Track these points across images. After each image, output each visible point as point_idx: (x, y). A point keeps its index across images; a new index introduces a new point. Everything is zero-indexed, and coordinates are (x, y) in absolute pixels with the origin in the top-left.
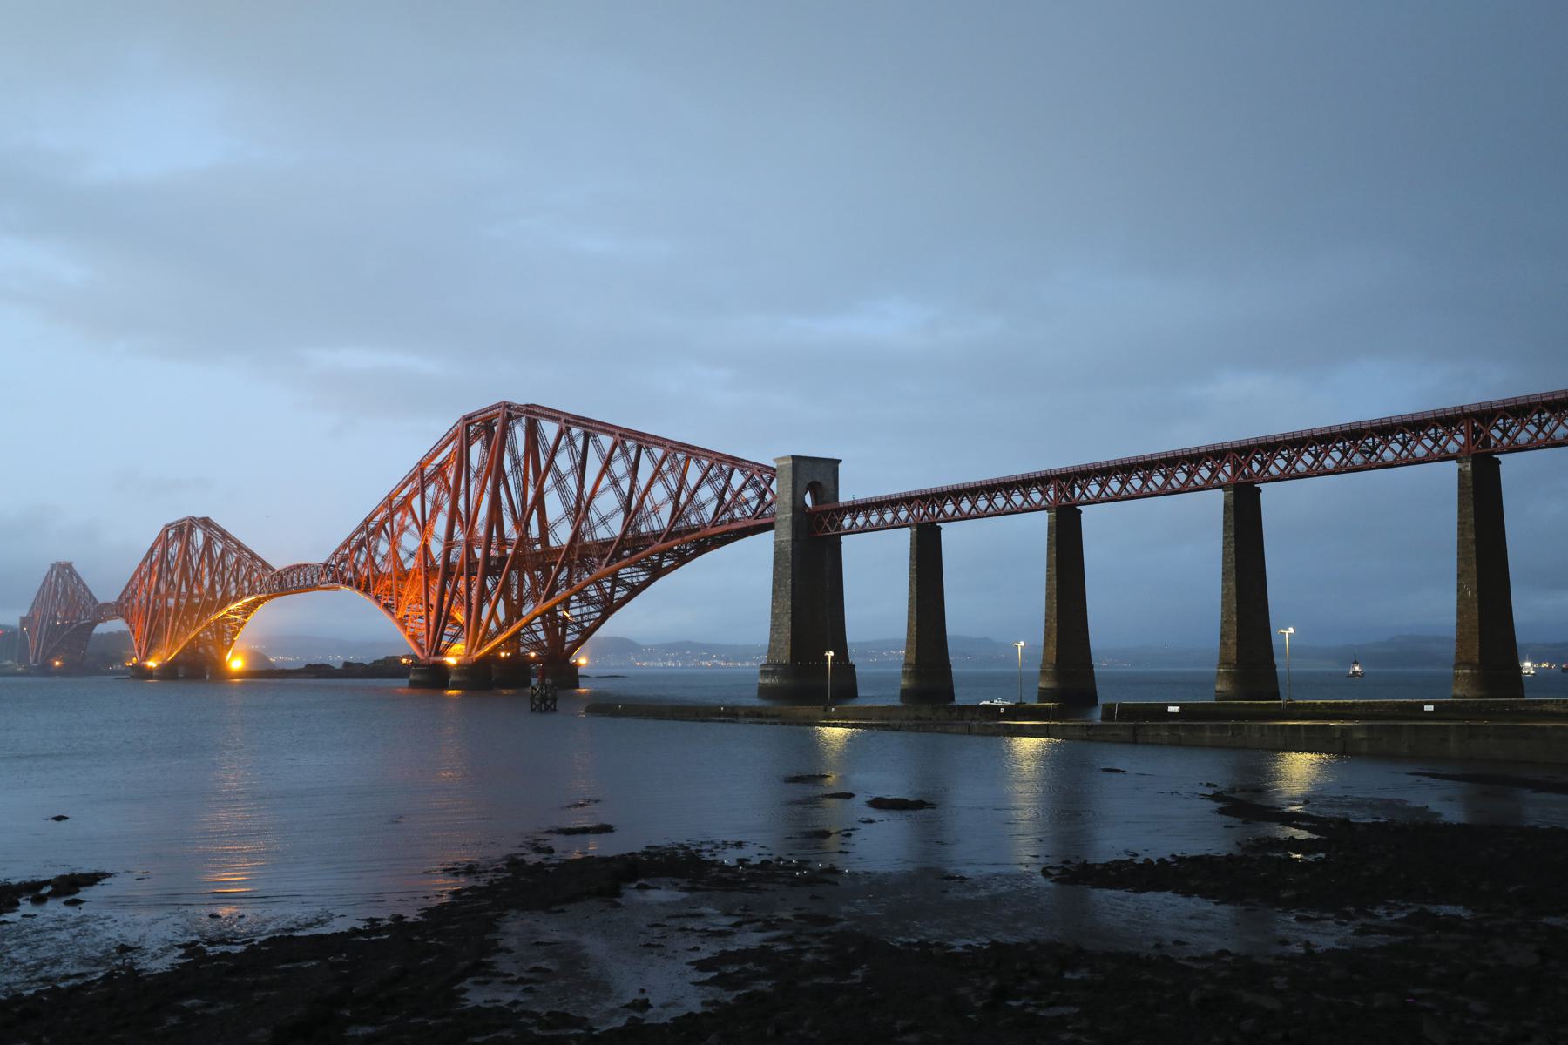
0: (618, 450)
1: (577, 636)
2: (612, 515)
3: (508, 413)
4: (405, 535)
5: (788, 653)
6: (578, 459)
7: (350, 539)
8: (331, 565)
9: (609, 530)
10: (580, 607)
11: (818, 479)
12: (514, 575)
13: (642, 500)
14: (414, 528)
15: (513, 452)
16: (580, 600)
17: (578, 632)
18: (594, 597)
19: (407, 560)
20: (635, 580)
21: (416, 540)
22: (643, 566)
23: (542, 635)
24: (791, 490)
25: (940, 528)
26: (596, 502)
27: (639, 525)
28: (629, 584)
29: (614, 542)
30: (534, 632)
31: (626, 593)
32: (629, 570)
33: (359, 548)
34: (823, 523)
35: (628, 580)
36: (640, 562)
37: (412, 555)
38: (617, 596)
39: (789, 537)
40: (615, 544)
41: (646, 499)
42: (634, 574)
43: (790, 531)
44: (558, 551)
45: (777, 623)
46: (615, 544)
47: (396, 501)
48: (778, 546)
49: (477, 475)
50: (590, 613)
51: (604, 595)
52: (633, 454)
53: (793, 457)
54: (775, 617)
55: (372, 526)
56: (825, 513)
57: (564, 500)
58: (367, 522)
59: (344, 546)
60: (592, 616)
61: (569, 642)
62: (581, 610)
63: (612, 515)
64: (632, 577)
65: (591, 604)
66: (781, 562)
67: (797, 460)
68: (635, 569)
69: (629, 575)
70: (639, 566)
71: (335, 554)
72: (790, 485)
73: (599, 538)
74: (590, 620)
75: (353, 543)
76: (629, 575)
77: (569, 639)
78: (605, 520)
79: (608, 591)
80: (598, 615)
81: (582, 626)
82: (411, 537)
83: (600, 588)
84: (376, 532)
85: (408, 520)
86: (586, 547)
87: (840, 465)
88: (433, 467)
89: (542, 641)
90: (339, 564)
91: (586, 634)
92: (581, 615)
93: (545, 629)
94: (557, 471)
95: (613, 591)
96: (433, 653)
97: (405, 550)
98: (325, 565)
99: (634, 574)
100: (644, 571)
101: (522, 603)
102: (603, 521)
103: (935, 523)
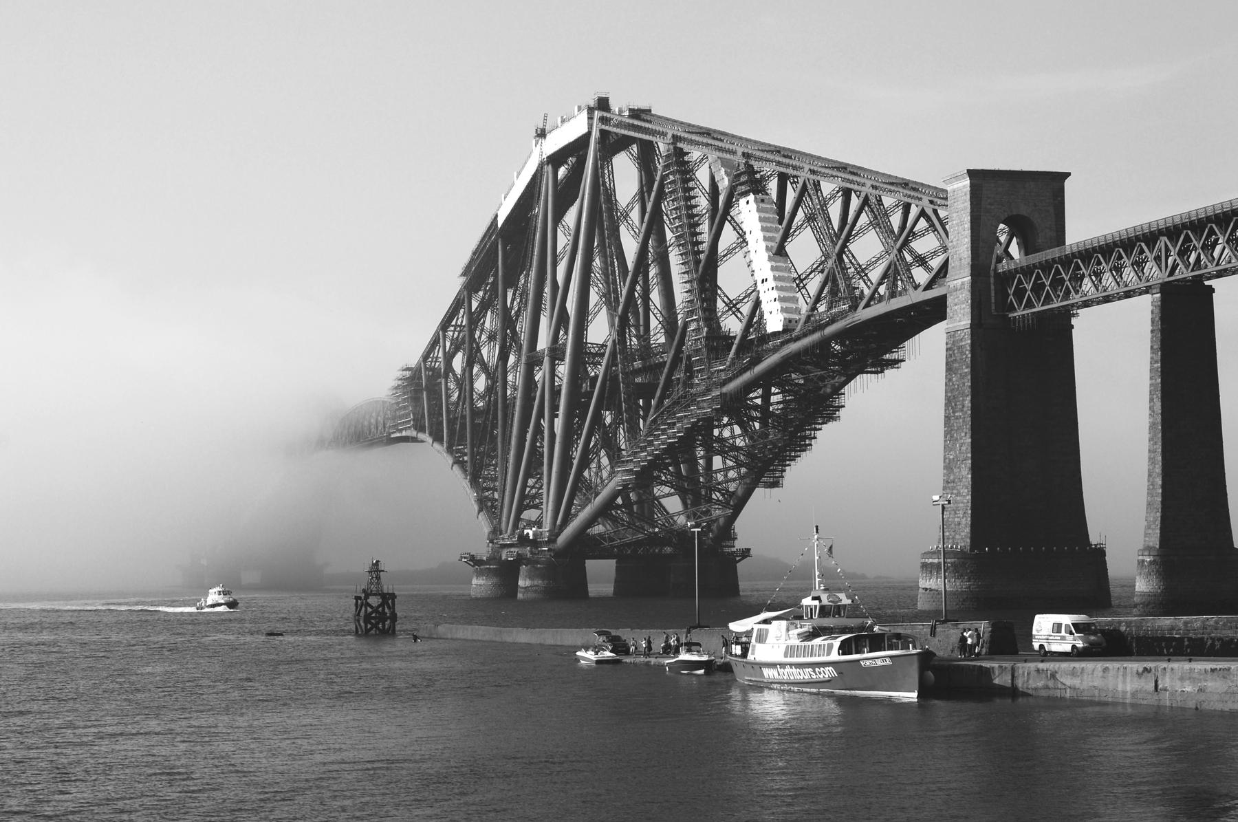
3: (602, 131)
5: (966, 531)
11: (1024, 210)
24: (968, 233)
25: (1211, 290)
34: (1026, 290)
39: (967, 321)
43: (968, 310)
45: (952, 477)
48: (951, 335)
53: (972, 174)
54: (949, 466)
56: (1046, 266)
66: (956, 365)
67: (978, 177)
72: (968, 225)
78: (735, 306)
87: (1068, 183)
91: (738, 503)
103: (1198, 280)
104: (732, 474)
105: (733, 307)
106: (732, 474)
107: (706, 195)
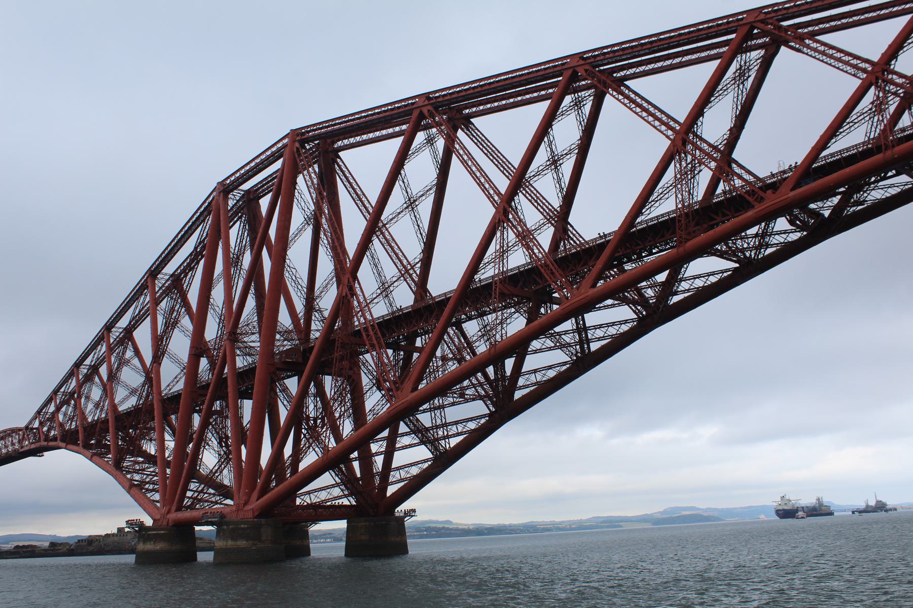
4: (125, 369)
7: (56, 392)
8: (32, 429)
14: (136, 362)
21: (138, 376)
33: (66, 402)
37: (133, 392)
47: (116, 333)
55: (85, 371)
58: (78, 364)
71: (39, 412)
82: (133, 373)
84: (89, 378)
85: (129, 354)
88: (167, 277)
96: (174, 508)
97: (126, 386)
98: (27, 428)
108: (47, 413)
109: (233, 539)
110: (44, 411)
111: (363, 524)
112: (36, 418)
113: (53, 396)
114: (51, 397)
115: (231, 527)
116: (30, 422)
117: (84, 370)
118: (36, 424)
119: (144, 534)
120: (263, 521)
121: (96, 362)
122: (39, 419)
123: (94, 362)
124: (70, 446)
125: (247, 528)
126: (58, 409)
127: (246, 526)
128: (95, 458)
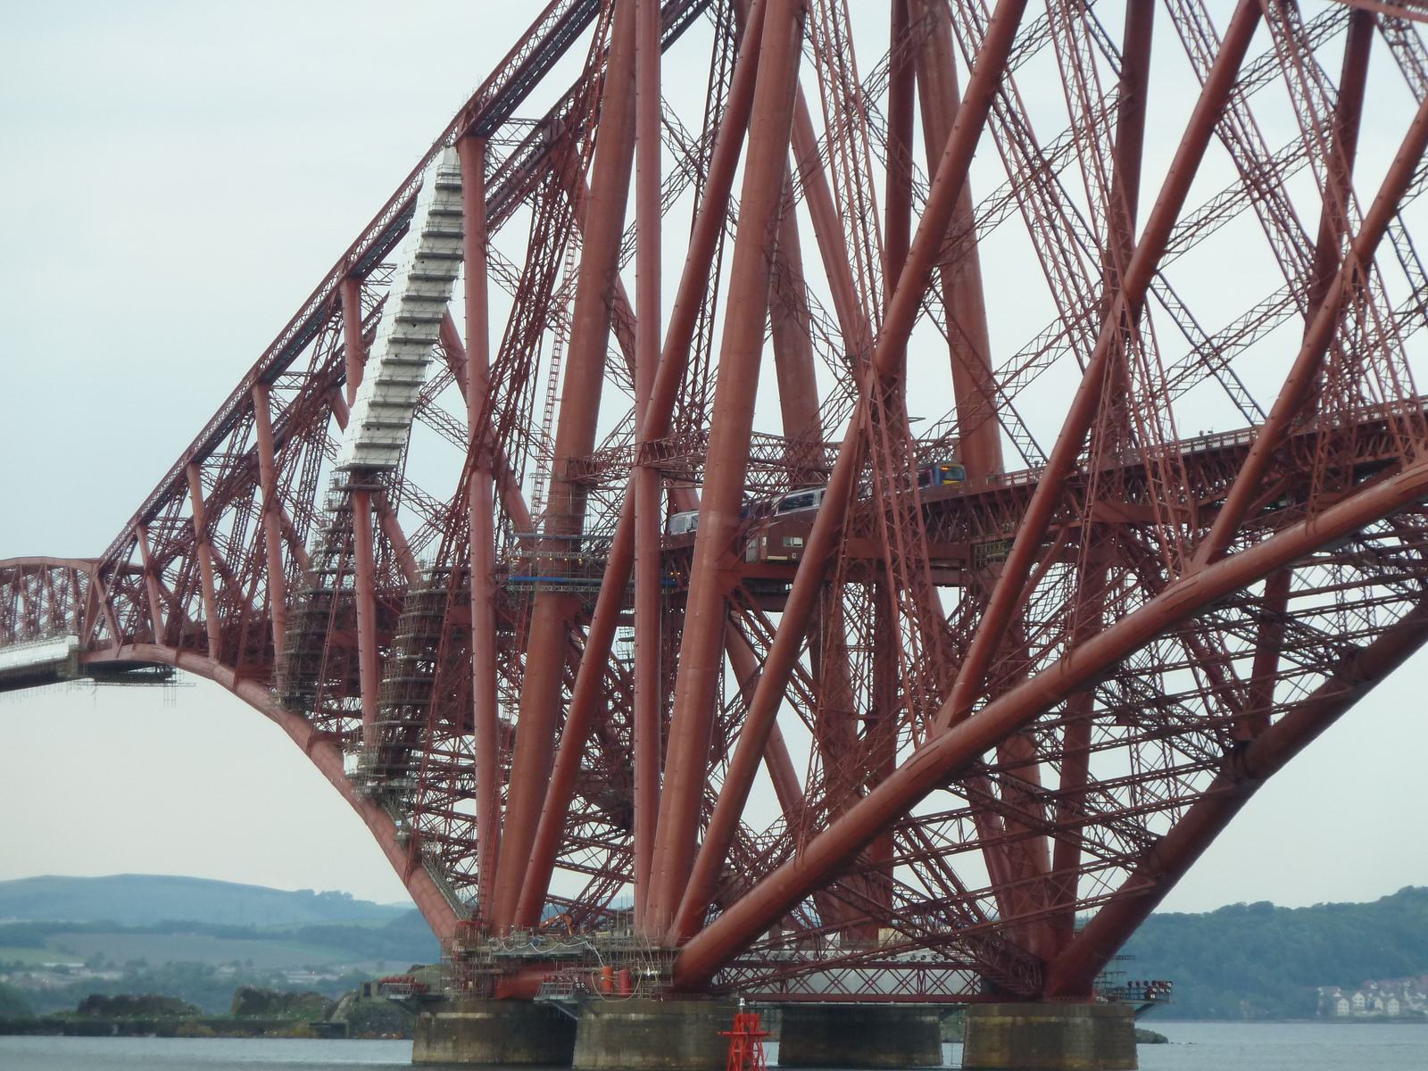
0: (1262, 40)
1: (1117, 878)
2: (1248, 330)
6: (1109, 81)
7: (196, 457)
8: (127, 570)
9: (1237, 394)
10: (1129, 741)
12: (853, 598)
13: (1365, 256)
15: (835, 53)
16: (1125, 715)
17: (1119, 860)
18: (1175, 700)
19: (423, 539)
20: (1354, 622)
22: (1380, 556)
23: (972, 870)
26: (1172, 268)
27: (1357, 371)
28: (1322, 639)
29: (1245, 449)
30: (930, 856)
31: (1316, 681)
32: (1316, 575)
33: (233, 489)
35: (1318, 623)
36: (1360, 539)
38: (1283, 693)
40: (1250, 461)
41: (1384, 252)
42: (1353, 595)
44: (1024, 492)
46: (1250, 461)
49: (693, 163)
50: (1170, 773)
51: (1221, 688)
52: (1331, 55)
57: (1056, 267)
58: (265, 374)
59: (175, 487)
60: (1183, 792)
61: (1090, 903)
62: (1135, 758)
63: (1248, 330)
64: (1341, 607)
65: (1163, 733)
68: (1348, 572)
69: (1329, 599)
70: (1357, 562)
71: (143, 520)
73: (1187, 431)
74: (1173, 803)
75: (213, 470)
76: (1329, 599)
77: (1087, 887)
78: (1217, 351)
79: (1244, 669)
80: (1203, 781)
81: (1140, 834)
83: (1212, 663)
86: (1135, 476)
88: (526, 131)
89: (972, 898)
90: (155, 568)
92: (1133, 781)
93: (989, 844)
94: (1020, 133)
95: (1266, 674)
98: (109, 569)
99: (1353, 595)
100: (1383, 580)
101: (883, 721)
102: (1211, 355)
104: (1159, 789)
105: (1211, 355)
106: (1159, 789)
107: (1116, 61)
108: (175, 519)
109: (611, 1049)
110: (162, 514)
111: (997, 1020)
112: (135, 539)
113: (190, 475)
114: (184, 473)
115: (607, 1016)
116: (117, 549)
117: (285, 393)
118: (137, 559)
119: (429, 1020)
120: (688, 1007)
121: (328, 363)
122: (145, 548)
123: (322, 359)
124: (249, 688)
125: (646, 1023)
126: (211, 512)
127: (641, 1017)
128: (320, 748)
